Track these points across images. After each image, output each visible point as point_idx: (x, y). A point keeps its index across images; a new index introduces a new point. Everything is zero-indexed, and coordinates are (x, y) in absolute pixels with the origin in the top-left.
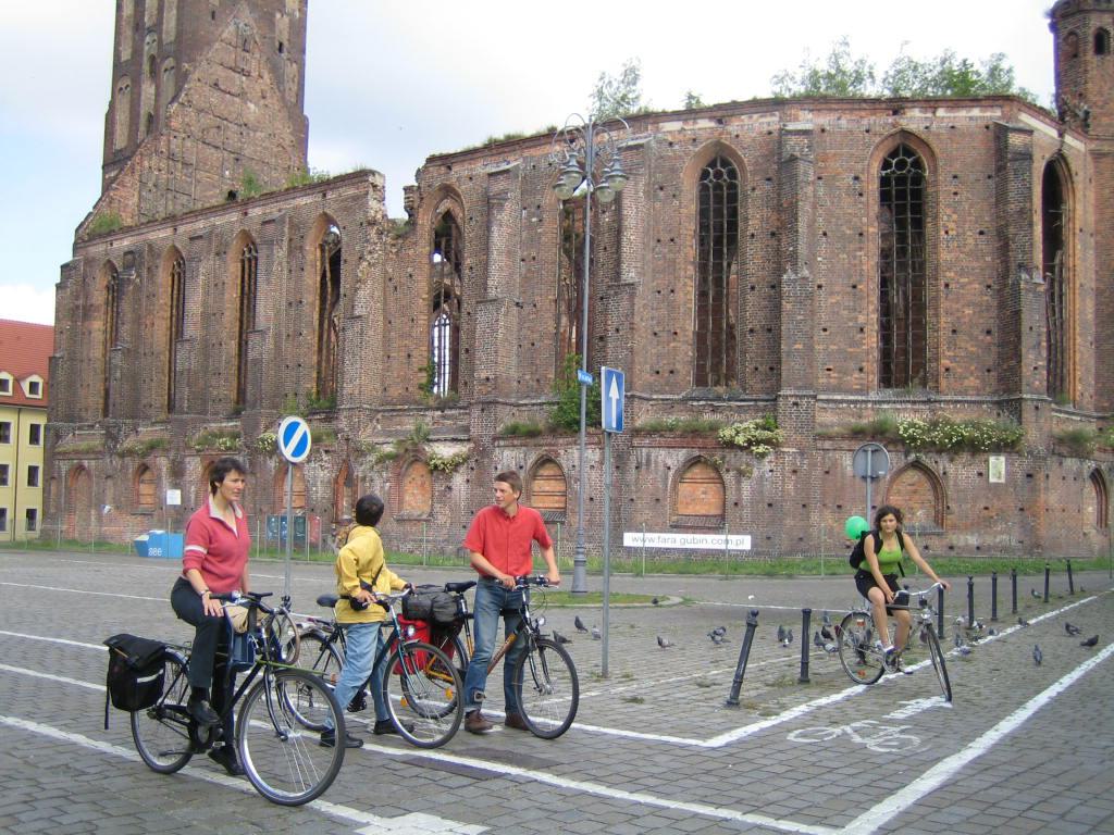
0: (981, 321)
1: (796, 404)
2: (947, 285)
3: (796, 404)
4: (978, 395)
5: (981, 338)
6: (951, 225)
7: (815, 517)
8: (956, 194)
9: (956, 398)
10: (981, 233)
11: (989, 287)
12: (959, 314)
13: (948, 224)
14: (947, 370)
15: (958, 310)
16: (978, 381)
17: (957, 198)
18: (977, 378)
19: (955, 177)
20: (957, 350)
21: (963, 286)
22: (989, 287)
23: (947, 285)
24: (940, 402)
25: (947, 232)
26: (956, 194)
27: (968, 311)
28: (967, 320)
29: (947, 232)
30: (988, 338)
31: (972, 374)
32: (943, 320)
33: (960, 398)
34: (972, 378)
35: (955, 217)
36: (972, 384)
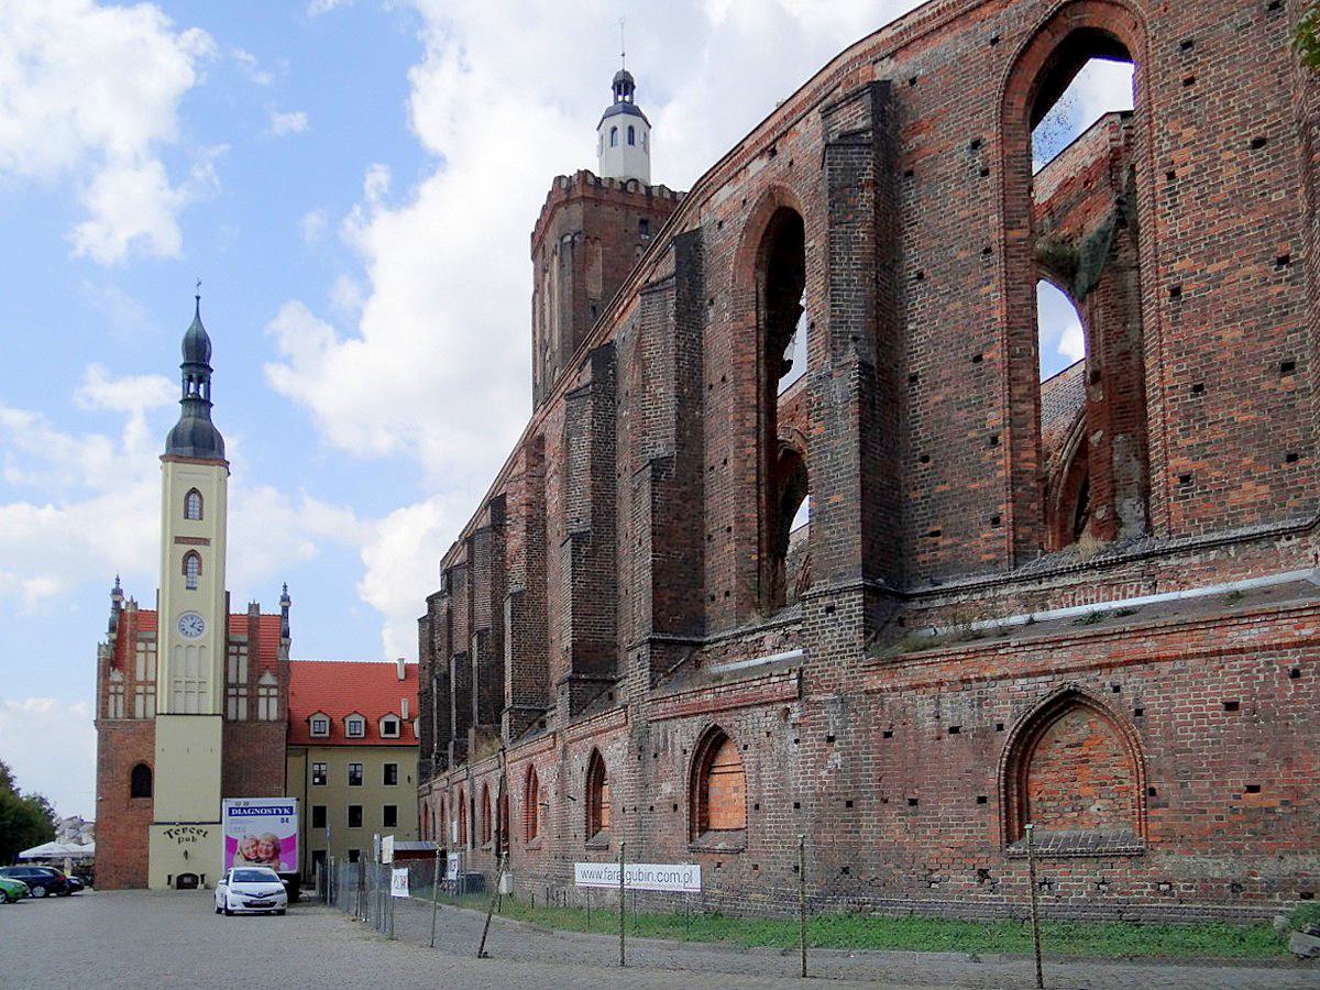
0: (1266, 346)
2: (1176, 292)
4: (1267, 521)
5: (1265, 386)
8: (1189, 82)
9: (1206, 538)
13: (1176, 156)
14: (1185, 479)
15: (1206, 338)
16: (1264, 489)
18: (1263, 481)
19: (1187, 45)
20: (1208, 431)
21: (1216, 281)
23: (1176, 292)
24: (1165, 554)
25: (1171, 176)
26: (1189, 82)
27: (1229, 334)
28: (1227, 355)
29: (1171, 176)
30: (1288, 380)
31: (1248, 476)
32: (1170, 369)
33: (1216, 536)
34: (1248, 485)
35: (1189, 133)
36: (1250, 499)
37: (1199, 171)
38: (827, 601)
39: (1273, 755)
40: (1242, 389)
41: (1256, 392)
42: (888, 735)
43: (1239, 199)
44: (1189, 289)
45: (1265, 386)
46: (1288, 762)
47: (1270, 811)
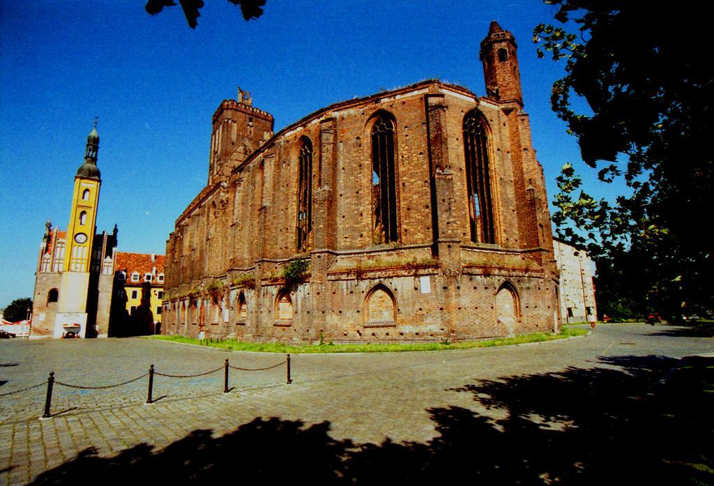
1: (319, 257)
3: (319, 257)
5: (422, 210)
6: (405, 152)
7: (328, 318)
8: (407, 136)
9: (410, 246)
10: (421, 153)
11: (426, 182)
12: (410, 199)
15: (410, 197)
17: (407, 138)
18: (422, 233)
21: (412, 183)
22: (426, 182)
23: (404, 184)
24: (401, 249)
25: (403, 157)
27: (415, 197)
29: (403, 157)
34: (419, 234)
35: (407, 148)
37: (408, 157)
38: (318, 255)
39: (424, 301)
40: (418, 211)
41: (420, 212)
42: (334, 293)
43: (416, 165)
44: (406, 184)
45: (422, 210)
46: (428, 303)
47: (424, 315)
